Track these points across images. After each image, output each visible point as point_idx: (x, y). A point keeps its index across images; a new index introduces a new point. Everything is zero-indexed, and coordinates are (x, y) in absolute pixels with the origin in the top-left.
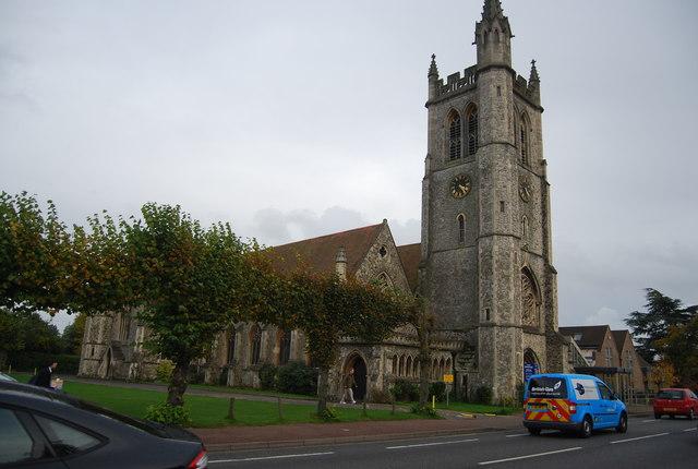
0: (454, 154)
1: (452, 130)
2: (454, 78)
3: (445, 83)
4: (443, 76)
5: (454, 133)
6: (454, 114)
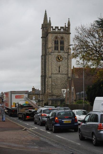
0: (56, 48)
1: (55, 42)
2: (57, 27)
3: (54, 28)
4: (53, 25)
5: (56, 42)
6: (56, 37)
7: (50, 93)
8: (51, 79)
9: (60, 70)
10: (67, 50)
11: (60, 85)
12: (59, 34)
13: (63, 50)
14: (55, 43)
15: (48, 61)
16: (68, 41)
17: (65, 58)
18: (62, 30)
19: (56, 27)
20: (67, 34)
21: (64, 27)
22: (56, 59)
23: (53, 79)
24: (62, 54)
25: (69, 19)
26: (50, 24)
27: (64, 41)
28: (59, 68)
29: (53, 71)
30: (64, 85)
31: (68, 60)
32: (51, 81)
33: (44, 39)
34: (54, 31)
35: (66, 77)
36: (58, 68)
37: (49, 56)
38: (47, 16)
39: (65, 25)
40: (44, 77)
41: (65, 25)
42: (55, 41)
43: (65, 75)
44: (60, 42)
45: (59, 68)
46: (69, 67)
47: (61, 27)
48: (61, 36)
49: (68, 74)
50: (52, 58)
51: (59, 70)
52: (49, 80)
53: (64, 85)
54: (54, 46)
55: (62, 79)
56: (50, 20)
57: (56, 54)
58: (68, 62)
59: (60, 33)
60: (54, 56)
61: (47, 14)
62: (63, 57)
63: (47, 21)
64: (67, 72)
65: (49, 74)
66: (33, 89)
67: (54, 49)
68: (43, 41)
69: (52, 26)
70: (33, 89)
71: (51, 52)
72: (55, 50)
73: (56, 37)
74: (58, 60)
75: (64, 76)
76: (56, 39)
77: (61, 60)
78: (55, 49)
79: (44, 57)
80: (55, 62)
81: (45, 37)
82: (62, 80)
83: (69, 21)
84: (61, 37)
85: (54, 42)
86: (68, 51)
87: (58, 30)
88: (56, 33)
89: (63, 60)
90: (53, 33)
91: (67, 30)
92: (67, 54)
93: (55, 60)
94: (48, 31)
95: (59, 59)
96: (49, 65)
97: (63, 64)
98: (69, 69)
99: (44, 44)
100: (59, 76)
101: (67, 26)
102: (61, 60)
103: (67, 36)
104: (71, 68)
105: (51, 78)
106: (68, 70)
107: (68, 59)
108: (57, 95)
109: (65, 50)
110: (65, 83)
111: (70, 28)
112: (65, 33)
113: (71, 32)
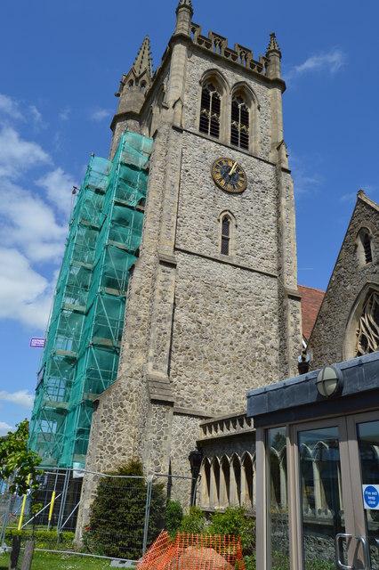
0: (209, 127)
5: (210, 102)
7: (152, 383)
9: (232, 243)
11: (228, 339)
14: (205, 104)
17: (261, 182)
25: (273, 35)
28: (226, 221)
29: (190, 238)
31: (278, 198)
35: (264, 292)
45: (226, 221)
46: (285, 234)
49: (278, 275)
51: (225, 240)
53: (257, 342)
55: (240, 299)
58: (278, 205)
74: (223, 182)
80: (205, 189)
82: (241, 305)
93: (203, 176)
96: (168, 186)
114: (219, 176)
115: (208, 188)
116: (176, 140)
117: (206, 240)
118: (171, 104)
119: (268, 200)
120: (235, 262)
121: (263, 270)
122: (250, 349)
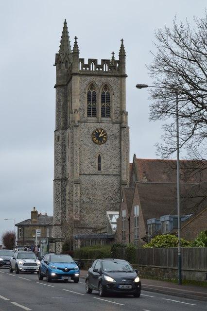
0: (92, 112)
1: (89, 96)
2: (93, 61)
3: (86, 62)
4: (85, 55)
5: (91, 98)
6: (92, 86)
7: (76, 222)
8: (79, 188)
9: (102, 166)
10: (117, 115)
11: (101, 203)
12: (99, 78)
13: (109, 116)
15: (73, 142)
16: (121, 94)
17: (113, 134)
18: (106, 68)
19: (90, 61)
20: (117, 76)
21: (109, 60)
22: (91, 139)
23: (83, 186)
24: (106, 125)
25: (122, 41)
26: (76, 52)
27: (111, 94)
30: (112, 201)
31: (120, 140)
32: (79, 192)
33: (62, 90)
34: (86, 69)
36: (97, 159)
37: (75, 130)
38: (69, 35)
39: (113, 57)
40: (61, 181)
41: (113, 57)
42: (88, 95)
43: (113, 178)
44: (100, 97)
46: (122, 158)
47: (103, 61)
48: (104, 81)
49: (120, 175)
50: (83, 134)
52: (75, 188)
53: (112, 201)
54: (86, 105)
56: (76, 42)
57: (92, 125)
58: (120, 144)
59: (101, 75)
60: (88, 132)
61: (69, 30)
62: (108, 133)
63: (68, 46)
64: (117, 170)
65: (74, 175)
66: (32, 212)
67: (86, 113)
68: (58, 94)
69: (81, 57)
70: (34, 213)
71: (79, 122)
72: (88, 116)
73: (92, 85)
74: (97, 141)
75: (111, 179)
76: (92, 88)
77: (104, 139)
78: (88, 114)
79: (60, 133)
81: (63, 86)
83: (122, 45)
84: (103, 83)
85: (86, 96)
86: (119, 117)
87: (97, 66)
88: (91, 75)
89: (108, 142)
90: (83, 75)
91: (116, 68)
92: (117, 126)
93: (88, 140)
94: (71, 71)
95: (99, 138)
96: (75, 152)
97: (107, 149)
98: (124, 164)
99: (62, 103)
100: (99, 179)
101: (117, 58)
102: (104, 139)
103: (119, 82)
104: (128, 159)
105: (79, 185)
106: (120, 165)
107: (120, 138)
108: (93, 225)
109: (114, 117)
110: (114, 196)
111: (124, 63)
112: (112, 76)
113: (127, 73)
114: (95, 139)
115: (91, 144)
116: (76, 131)
117: (92, 167)
118: (74, 111)
119: (117, 142)
120: (103, 173)
121: (115, 173)
122: (109, 205)
